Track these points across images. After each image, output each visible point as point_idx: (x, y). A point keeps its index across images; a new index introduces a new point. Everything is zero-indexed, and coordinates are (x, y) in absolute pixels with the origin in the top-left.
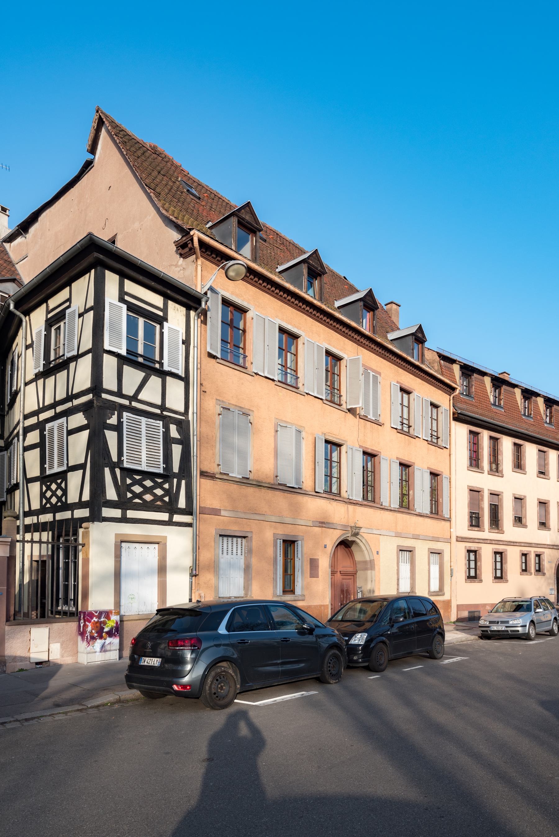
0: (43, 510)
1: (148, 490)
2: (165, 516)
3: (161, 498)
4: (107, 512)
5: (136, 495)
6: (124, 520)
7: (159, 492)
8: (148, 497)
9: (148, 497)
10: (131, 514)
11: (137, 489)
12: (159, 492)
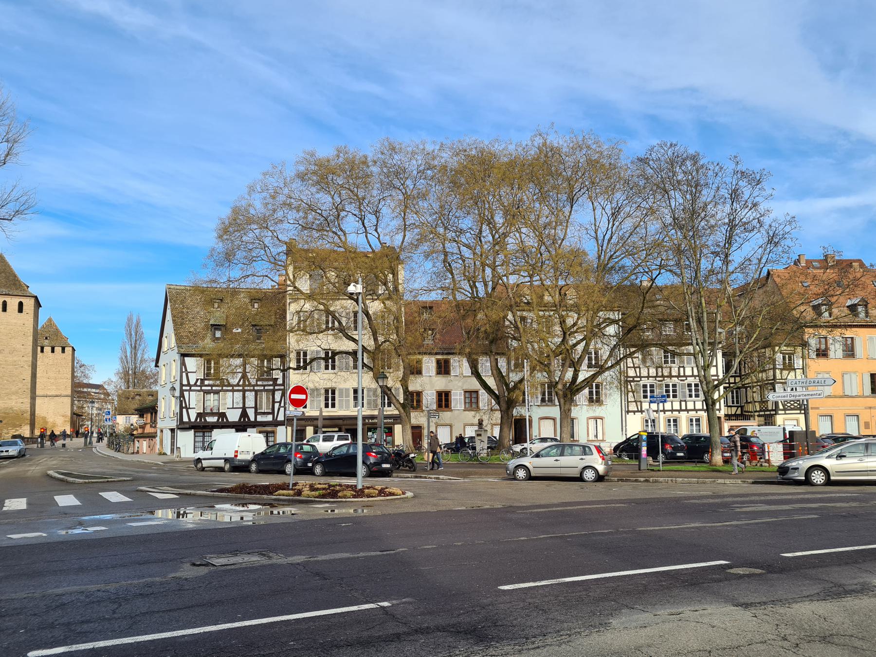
0: (761, 411)
1: (792, 405)
2: (799, 412)
3: (796, 406)
4: (780, 412)
5: (788, 407)
6: (785, 414)
7: (796, 405)
8: (792, 407)
9: (792, 407)
10: (787, 412)
11: (789, 405)
12: (796, 405)
